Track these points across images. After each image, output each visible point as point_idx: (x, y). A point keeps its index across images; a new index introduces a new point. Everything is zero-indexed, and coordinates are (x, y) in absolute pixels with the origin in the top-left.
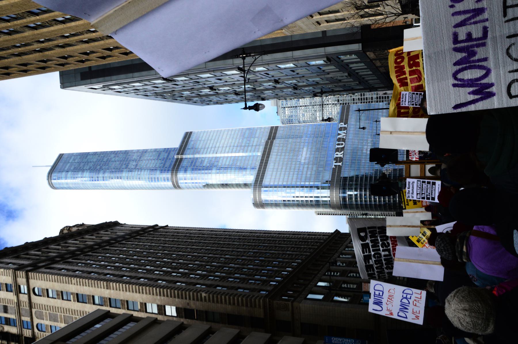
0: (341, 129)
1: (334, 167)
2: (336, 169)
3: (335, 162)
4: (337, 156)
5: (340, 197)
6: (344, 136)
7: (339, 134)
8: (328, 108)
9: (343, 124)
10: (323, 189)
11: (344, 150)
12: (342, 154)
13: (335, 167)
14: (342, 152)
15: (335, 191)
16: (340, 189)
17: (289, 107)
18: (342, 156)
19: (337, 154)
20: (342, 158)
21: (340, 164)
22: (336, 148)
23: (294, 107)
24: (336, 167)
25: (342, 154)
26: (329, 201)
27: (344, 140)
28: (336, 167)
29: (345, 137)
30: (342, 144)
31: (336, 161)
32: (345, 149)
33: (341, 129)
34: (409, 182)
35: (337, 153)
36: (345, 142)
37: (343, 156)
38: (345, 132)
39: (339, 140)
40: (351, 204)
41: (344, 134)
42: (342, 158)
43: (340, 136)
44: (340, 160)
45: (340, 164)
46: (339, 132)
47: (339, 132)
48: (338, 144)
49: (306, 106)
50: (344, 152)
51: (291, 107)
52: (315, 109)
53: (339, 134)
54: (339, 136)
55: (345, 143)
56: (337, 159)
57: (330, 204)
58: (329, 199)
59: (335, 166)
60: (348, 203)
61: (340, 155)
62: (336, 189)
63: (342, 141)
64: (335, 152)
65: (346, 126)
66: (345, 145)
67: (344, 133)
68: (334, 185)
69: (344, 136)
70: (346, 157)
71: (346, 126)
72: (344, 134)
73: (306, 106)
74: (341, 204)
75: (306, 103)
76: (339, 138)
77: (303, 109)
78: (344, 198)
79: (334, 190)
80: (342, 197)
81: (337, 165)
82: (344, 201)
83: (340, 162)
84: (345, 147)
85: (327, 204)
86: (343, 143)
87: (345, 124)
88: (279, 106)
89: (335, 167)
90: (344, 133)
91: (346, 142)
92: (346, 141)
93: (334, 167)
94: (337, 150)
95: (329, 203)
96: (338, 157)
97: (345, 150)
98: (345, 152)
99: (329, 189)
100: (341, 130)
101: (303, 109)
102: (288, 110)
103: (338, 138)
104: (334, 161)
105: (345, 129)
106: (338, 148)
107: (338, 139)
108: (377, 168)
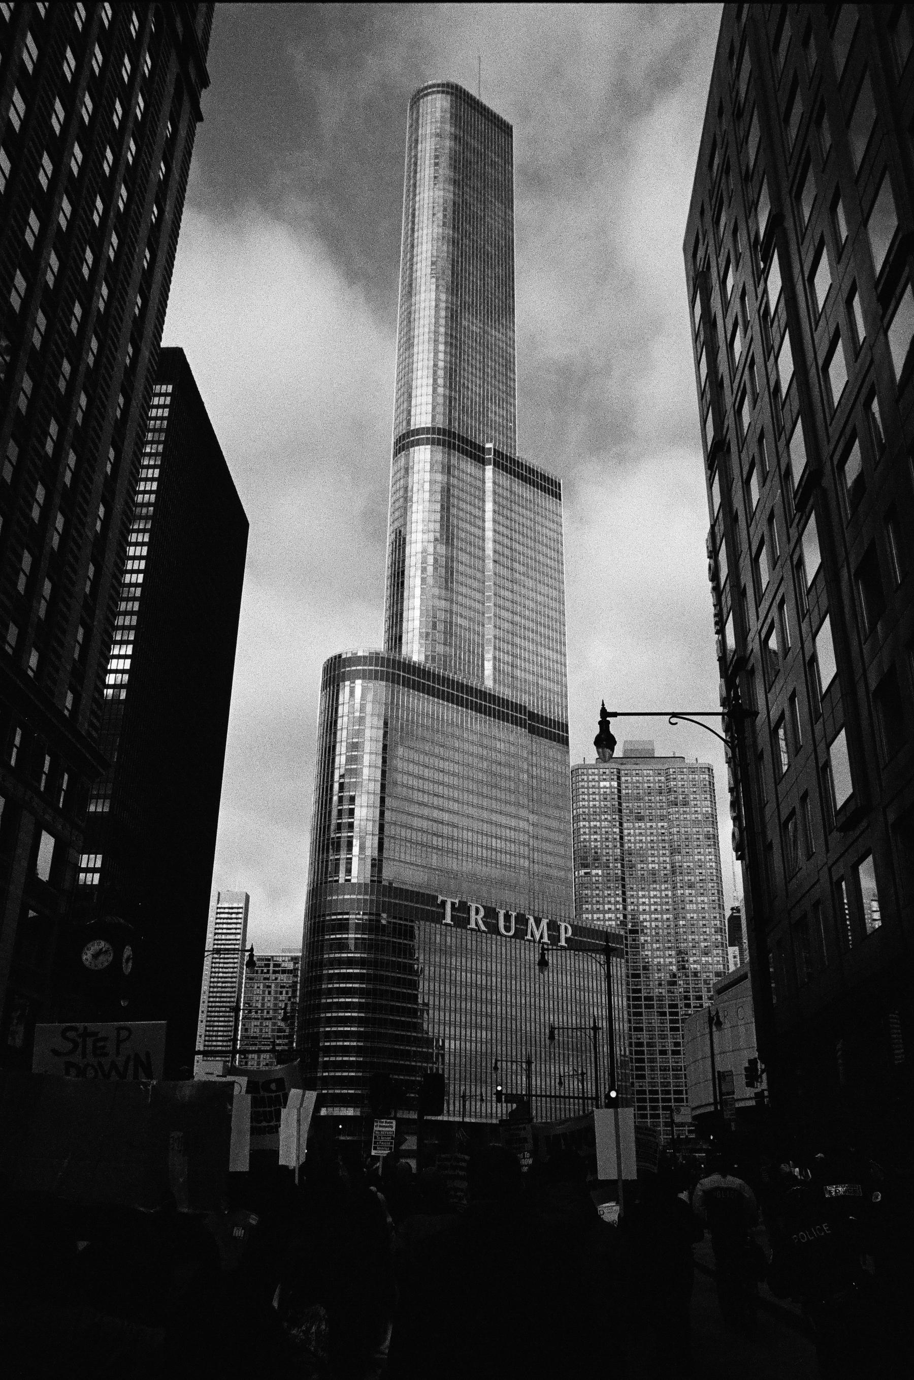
0: (553, 926)
1: (440, 898)
2: (432, 906)
3: (453, 904)
4: (473, 913)
5: (347, 913)
6: (532, 935)
7: (538, 921)
8: (613, 900)
10: (373, 866)
11: (489, 932)
12: (477, 924)
13: (439, 902)
14: (483, 928)
15: (365, 900)
16: (371, 914)
17: (619, 791)
18: (473, 925)
19: (477, 913)
20: (465, 928)
21: (448, 920)
22: (497, 910)
23: (620, 804)
24: (438, 906)
25: (477, 924)
26: (337, 881)
27: (520, 934)
28: (438, 906)
29: (529, 937)
30: (508, 929)
31: (457, 906)
33: (553, 926)
34: (392, 1123)
35: (482, 912)
37: (472, 930)
38: (546, 940)
39: (522, 920)
40: (322, 946)
41: (538, 937)
42: (465, 928)
43: (534, 924)
44: (461, 920)
45: (448, 920)
46: (544, 923)
47: (544, 923)
48: (507, 917)
49: (621, 838)
50: (484, 932)
51: (620, 798)
52: (611, 865)
53: (538, 921)
54: (532, 920)
55: (511, 937)
56: (463, 908)
57: (326, 883)
58: (341, 881)
59: (444, 903)
60: (327, 937)
61: (476, 919)
62: (372, 901)
63: (516, 927)
64: (483, 906)
65: (563, 943)
66: (506, 936)
67: (541, 937)
68: (384, 896)
69: (532, 935)
70: (469, 938)
71: (563, 943)
72: (538, 937)
73: (621, 838)
74: (324, 915)
75: (629, 841)
76: (527, 920)
77: (615, 830)
78: (343, 926)
79: (368, 897)
80: (347, 919)
82: (334, 926)
84: (499, 937)
85: (326, 874)
87: (567, 940)
88: (622, 764)
89: (439, 902)
90: (541, 937)
91: (513, 940)
92: (518, 941)
93: (440, 898)
94: (491, 913)
95: (330, 879)
96: (469, 914)
98: (484, 935)
99: (372, 881)
100: (549, 929)
101: (615, 830)
102: (611, 787)
103: (527, 916)
104: (457, 901)
105: (555, 939)
106: (496, 915)
108: (421, 987)
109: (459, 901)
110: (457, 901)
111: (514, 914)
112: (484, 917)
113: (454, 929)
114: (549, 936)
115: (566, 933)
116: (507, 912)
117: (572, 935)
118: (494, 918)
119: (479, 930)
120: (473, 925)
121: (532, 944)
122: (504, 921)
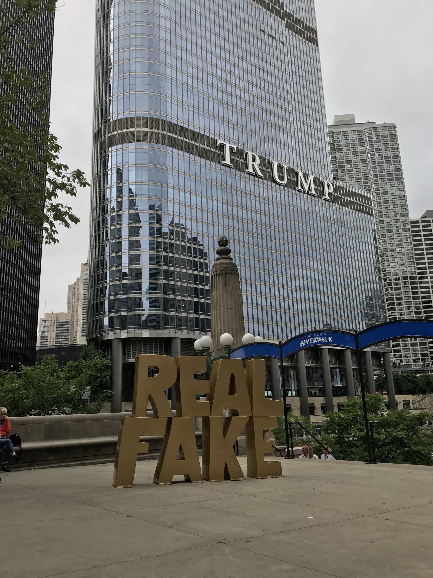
1: (219, 142)
3: (231, 149)
6: (302, 187)
7: (306, 176)
9: (331, 190)
11: (265, 178)
12: (254, 169)
14: (260, 173)
19: (254, 159)
20: (244, 171)
25: (254, 169)
30: (282, 179)
31: (235, 151)
32: (269, 183)
35: (258, 161)
36: (288, 185)
38: (313, 192)
39: (293, 173)
41: (307, 189)
46: (311, 178)
47: (311, 178)
48: (280, 168)
50: (260, 177)
53: (306, 176)
54: (301, 175)
55: (284, 186)
59: (222, 146)
63: (287, 178)
64: (259, 156)
67: (309, 189)
69: (302, 187)
71: (327, 197)
72: (307, 189)
76: (297, 173)
81: (223, 151)
83: (232, 160)
84: (274, 184)
86: (285, 182)
87: (330, 194)
90: (309, 189)
91: (286, 188)
92: (290, 190)
93: (219, 142)
97: (265, 182)
98: (261, 180)
100: (315, 184)
105: (320, 194)
106: (270, 165)
107: (293, 170)
109: (237, 149)
110: (235, 147)
111: (286, 167)
112: (260, 165)
113: (233, 171)
114: (316, 190)
115: (328, 189)
116: (280, 164)
117: (333, 191)
118: (269, 168)
119: (257, 175)
120: (251, 170)
121: (302, 194)
122: (278, 172)
